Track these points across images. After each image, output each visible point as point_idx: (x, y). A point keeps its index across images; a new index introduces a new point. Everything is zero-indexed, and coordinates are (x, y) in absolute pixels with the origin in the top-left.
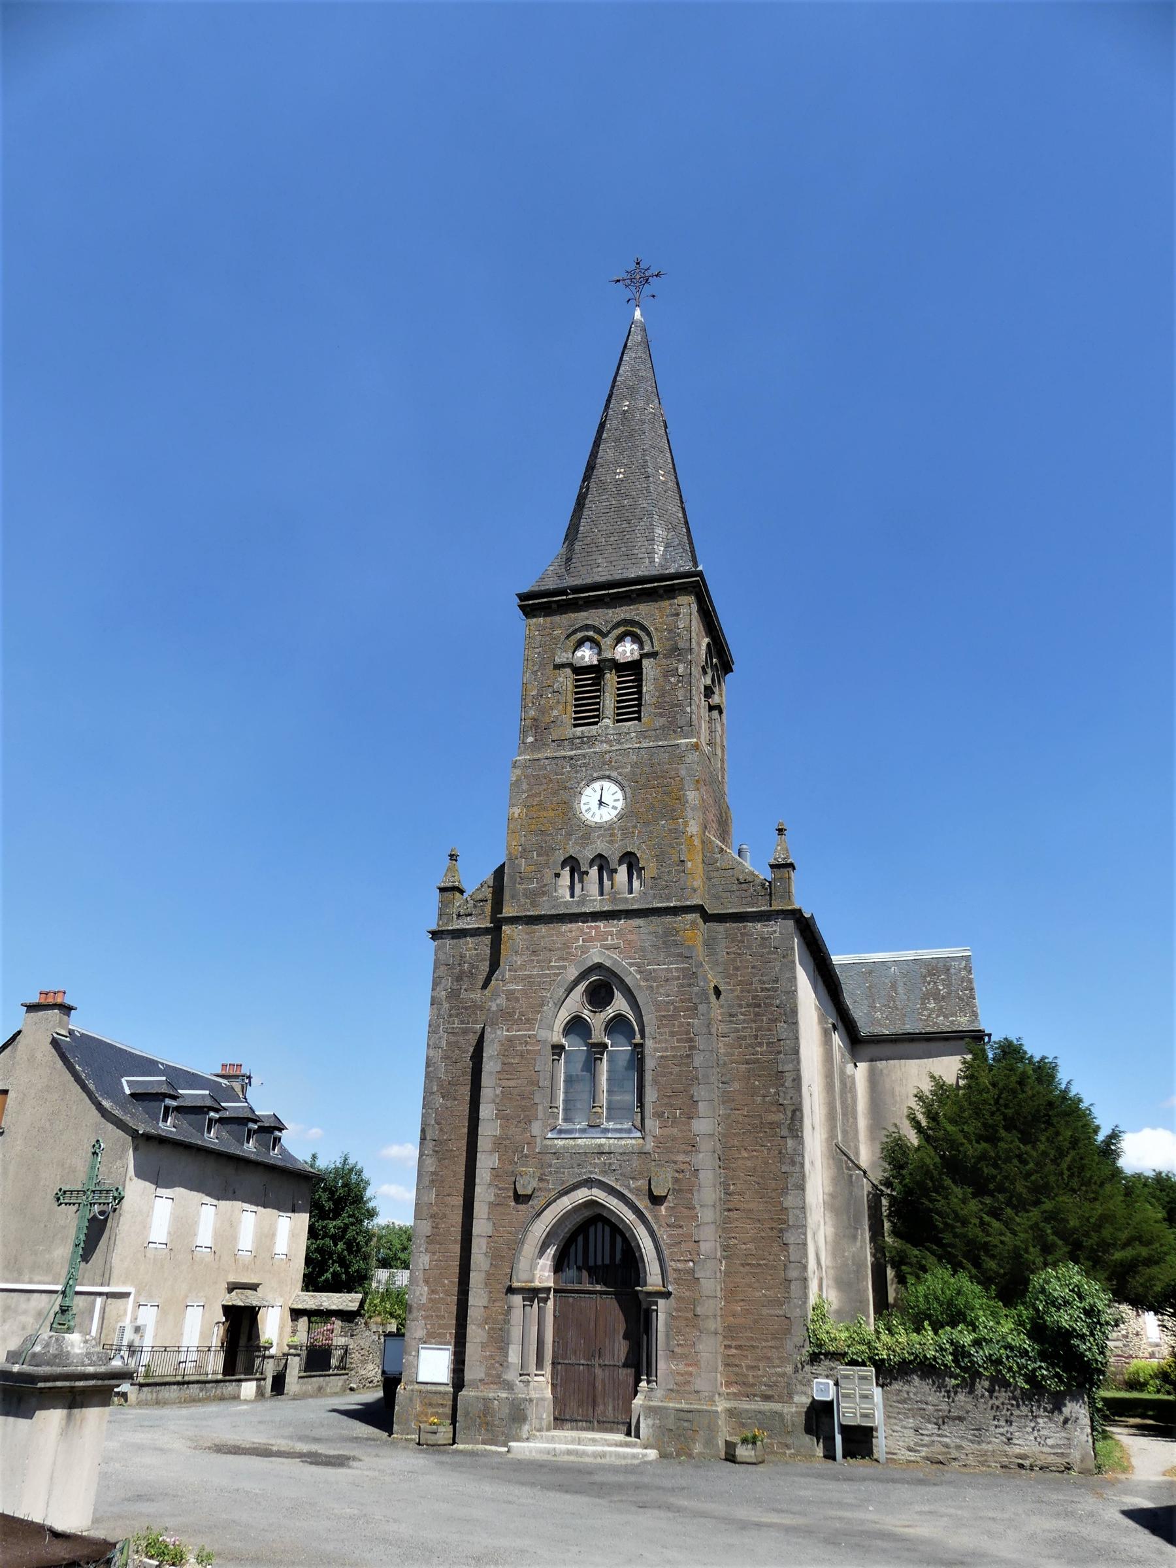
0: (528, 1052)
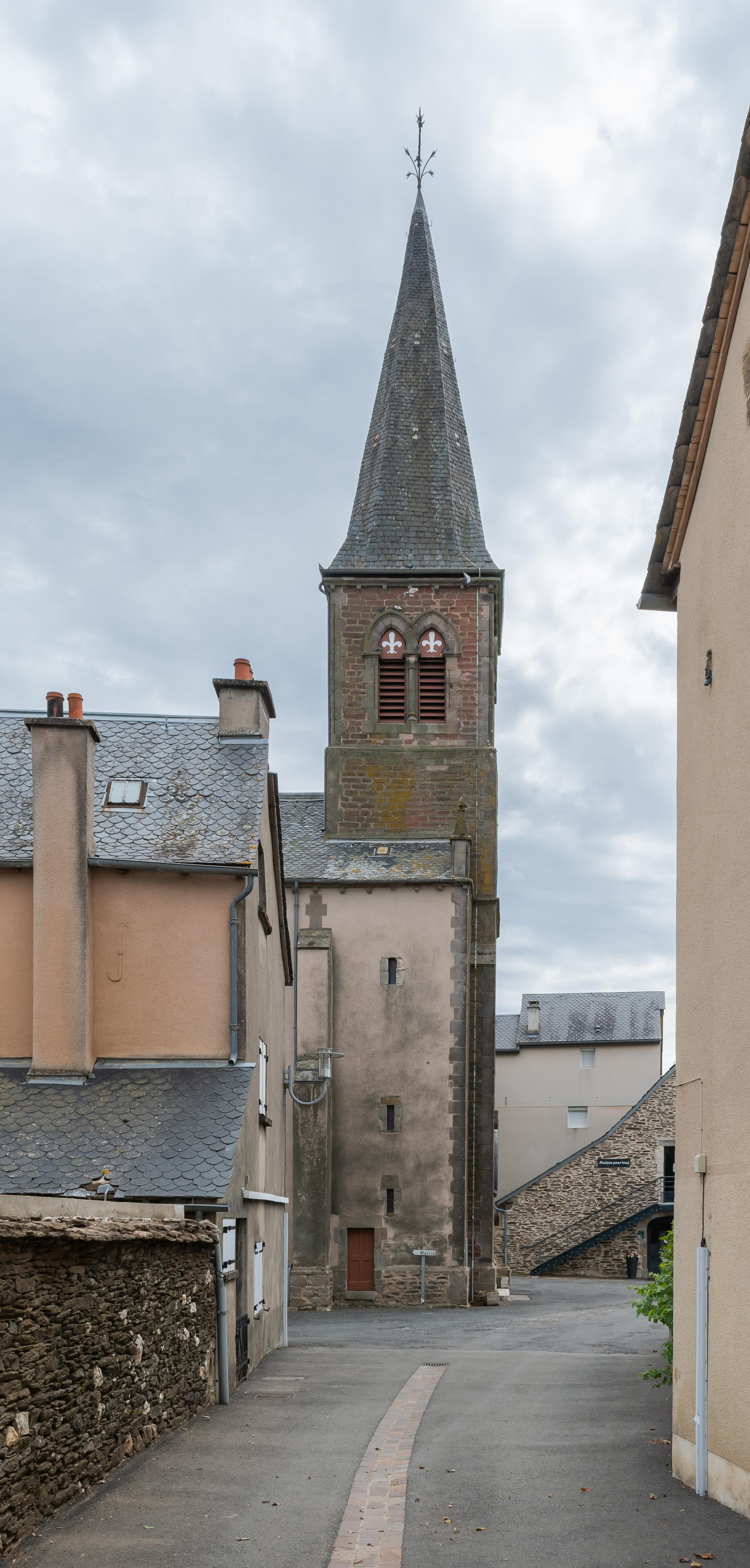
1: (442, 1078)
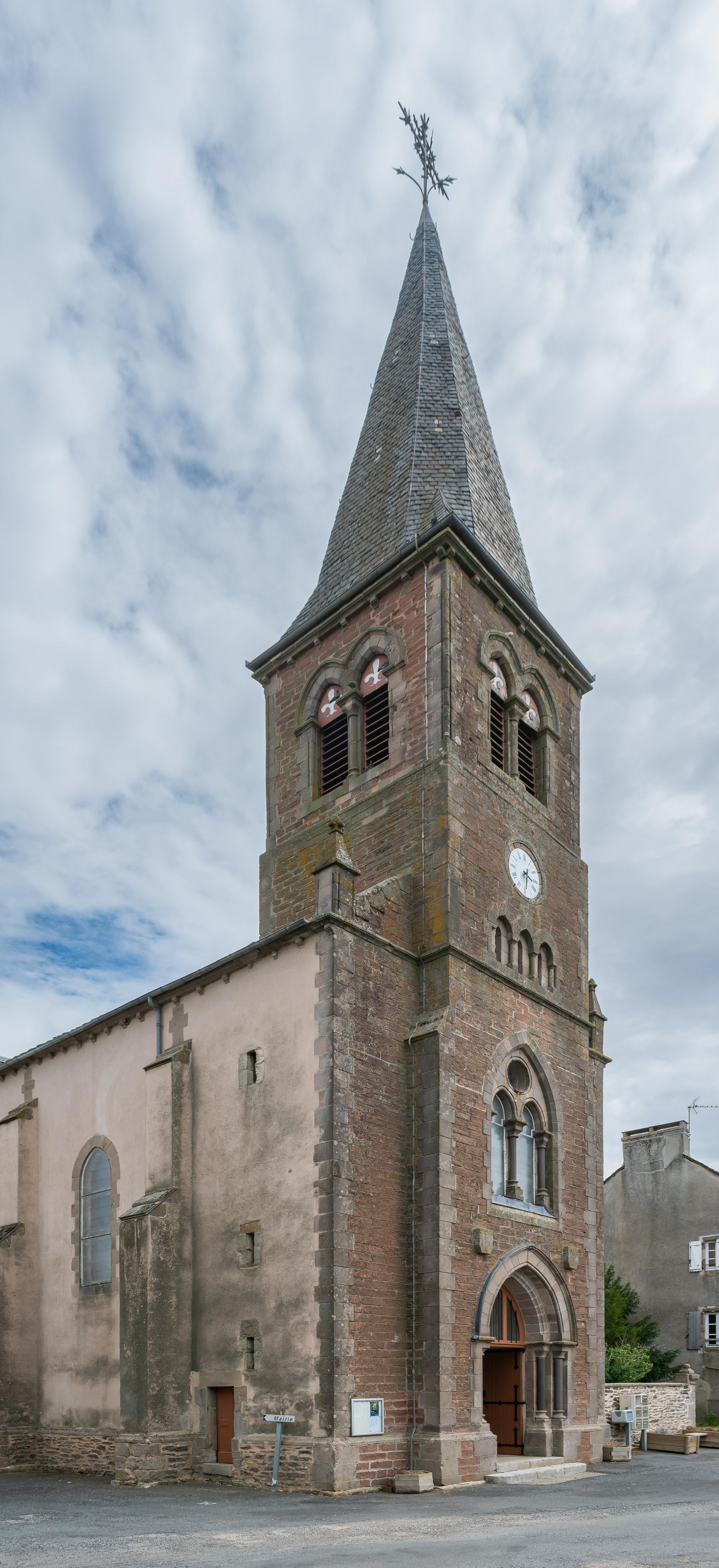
1: (306, 1187)
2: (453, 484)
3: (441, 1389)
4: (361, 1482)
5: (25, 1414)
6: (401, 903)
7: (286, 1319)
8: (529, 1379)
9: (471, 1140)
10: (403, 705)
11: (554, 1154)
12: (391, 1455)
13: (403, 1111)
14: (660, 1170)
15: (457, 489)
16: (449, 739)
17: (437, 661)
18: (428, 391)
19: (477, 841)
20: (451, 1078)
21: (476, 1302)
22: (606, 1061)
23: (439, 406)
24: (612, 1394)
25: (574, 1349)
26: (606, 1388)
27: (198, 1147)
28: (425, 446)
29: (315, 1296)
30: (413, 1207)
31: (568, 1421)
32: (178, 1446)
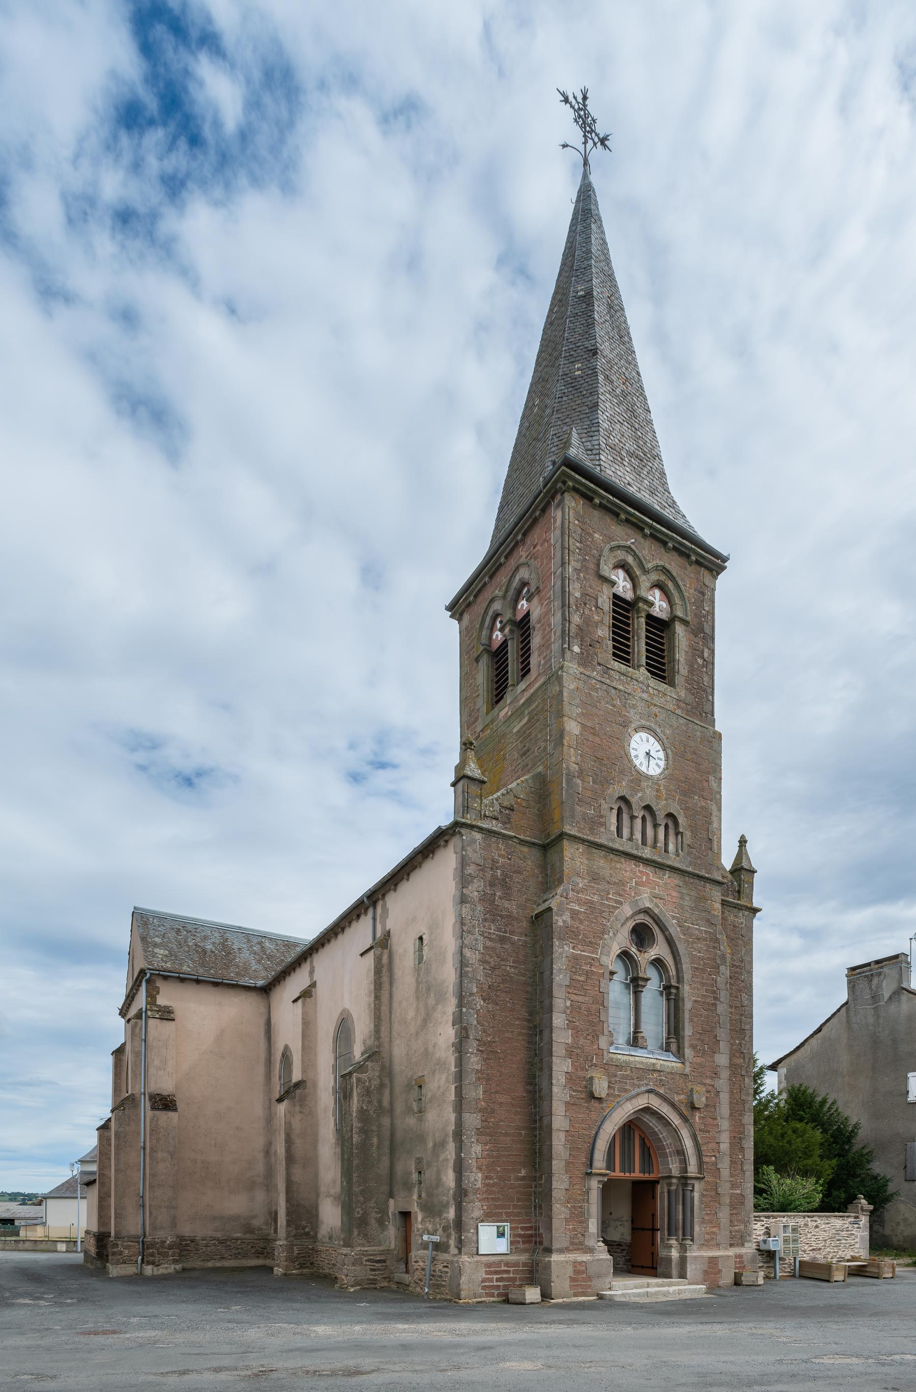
0: (593, 973)
1: (448, 1047)
2: (586, 419)
3: (554, 1216)
4: (486, 1293)
5: (307, 1230)
6: (531, 799)
7: (437, 1156)
8: (662, 1208)
9: (586, 998)
10: (539, 626)
11: (681, 1003)
12: (515, 1272)
13: (530, 978)
14: (881, 1003)
15: (588, 423)
16: (567, 650)
17: (559, 583)
18: (572, 340)
19: (594, 734)
20: (565, 946)
21: (591, 1140)
22: (755, 911)
23: (580, 351)
24: (763, 1223)
25: (702, 1182)
26: (755, 1217)
27: (393, 1016)
28: (566, 391)
29: (453, 1137)
30: (537, 1059)
31: (695, 1247)
32: (378, 1259)
